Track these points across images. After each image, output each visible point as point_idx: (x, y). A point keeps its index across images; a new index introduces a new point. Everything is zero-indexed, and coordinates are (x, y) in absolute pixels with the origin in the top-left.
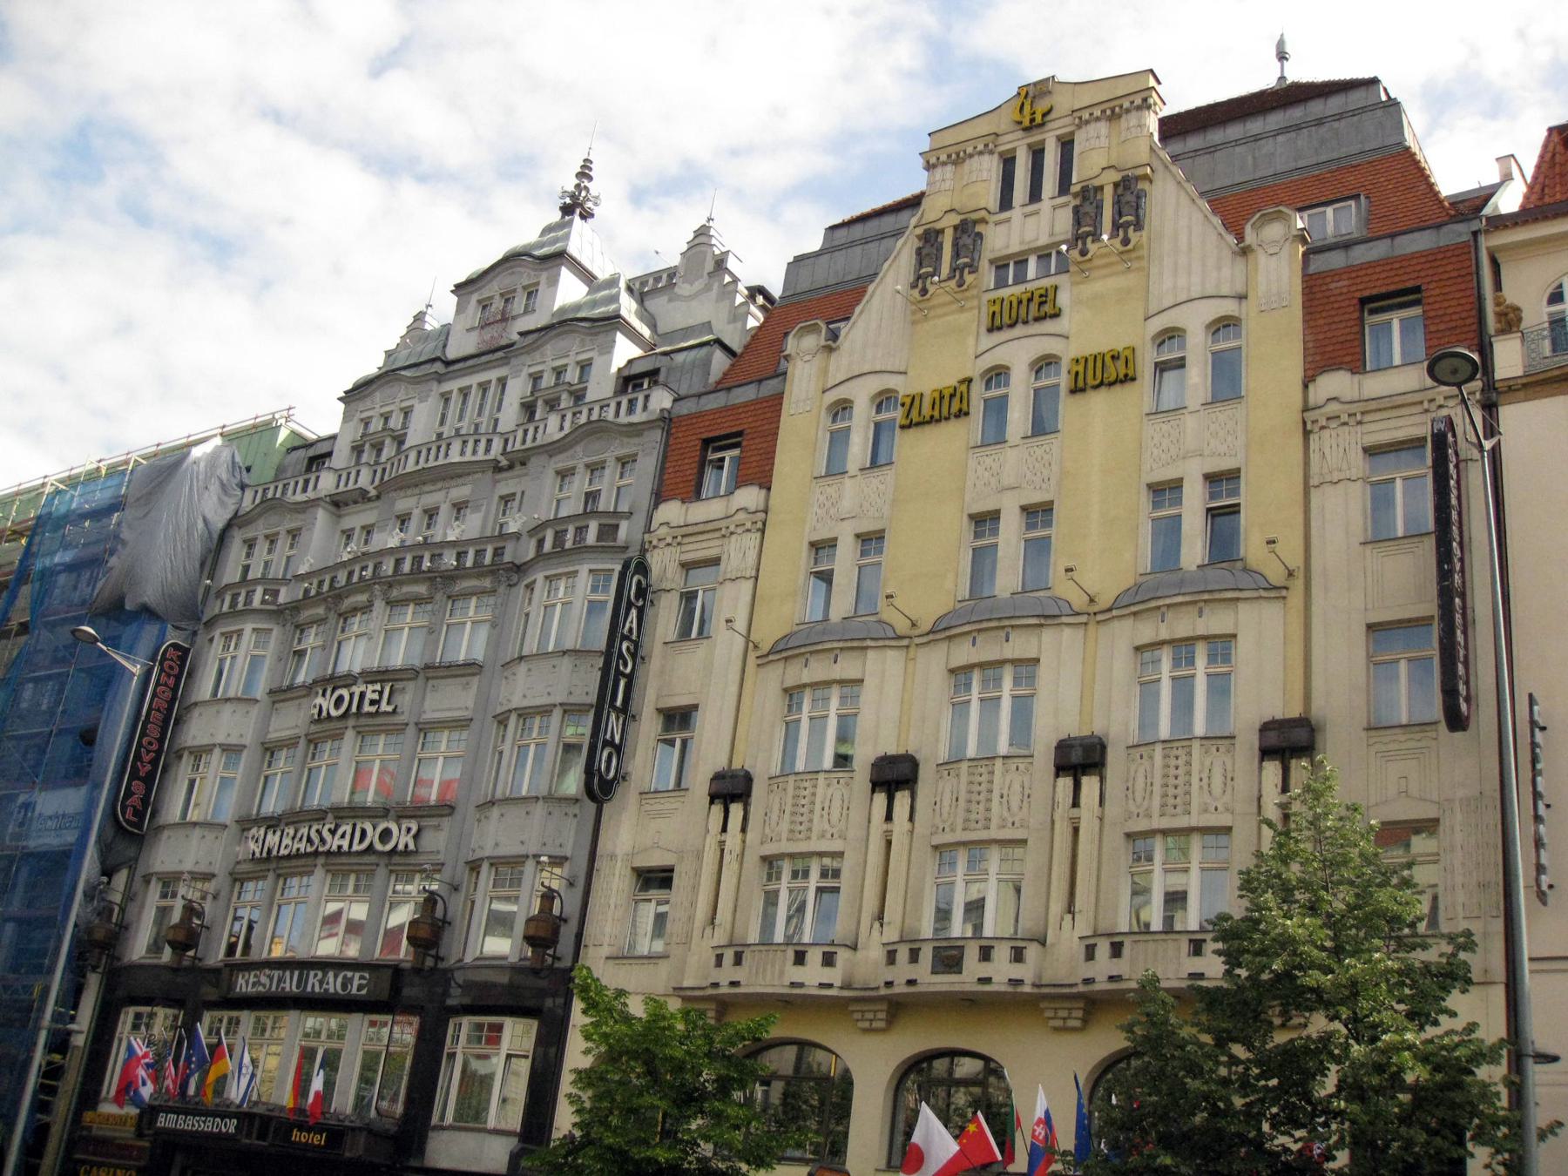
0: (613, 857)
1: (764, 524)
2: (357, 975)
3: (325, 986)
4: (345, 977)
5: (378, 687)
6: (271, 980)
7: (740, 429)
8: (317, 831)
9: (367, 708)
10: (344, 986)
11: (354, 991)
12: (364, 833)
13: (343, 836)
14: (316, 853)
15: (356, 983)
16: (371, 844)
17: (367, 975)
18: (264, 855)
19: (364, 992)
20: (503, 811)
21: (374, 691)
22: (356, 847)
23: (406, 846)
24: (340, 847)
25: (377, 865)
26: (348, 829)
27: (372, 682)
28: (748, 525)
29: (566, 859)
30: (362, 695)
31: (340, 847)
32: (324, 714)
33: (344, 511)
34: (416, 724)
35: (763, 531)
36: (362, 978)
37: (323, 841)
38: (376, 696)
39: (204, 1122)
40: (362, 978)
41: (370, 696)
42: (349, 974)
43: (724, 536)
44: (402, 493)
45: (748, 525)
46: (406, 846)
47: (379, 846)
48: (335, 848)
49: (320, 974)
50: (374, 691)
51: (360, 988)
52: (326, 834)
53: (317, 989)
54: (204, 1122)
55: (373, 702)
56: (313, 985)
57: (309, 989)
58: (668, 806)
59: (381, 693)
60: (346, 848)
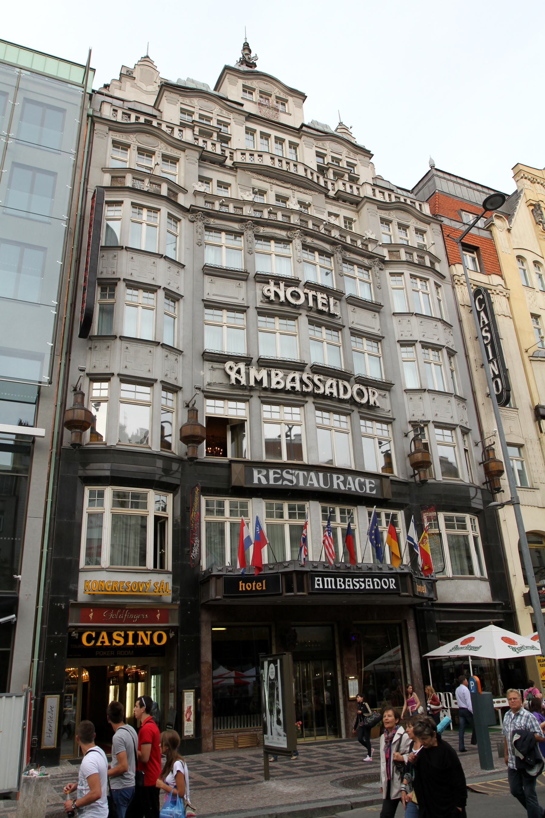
2: (367, 481)
3: (348, 486)
4: (359, 480)
6: (297, 477)
10: (361, 488)
11: (368, 491)
13: (331, 386)
15: (368, 486)
16: (352, 396)
17: (373, 481)
18: (252, 383)
19: (374, 492)
20: (411, 396)
22: (342, 396)
23: (375, 403)
25: (353, 411)
30: (315, 299)
31: (331, 393)
36: (370, 483)
37: (318, 388)
39: (364, 582)
40: (370, 483)
41: (320, 301)
42: (362, 480)
46: (375, 403)
47: (357, 399)
49: (342, 478)
50: (322, 298)
51: (371, 489)
53: (342, 487)
54: (364, 582)
55: (323, 304)
56: (338, 484)
57: (335, 487)
60: (335, 394)
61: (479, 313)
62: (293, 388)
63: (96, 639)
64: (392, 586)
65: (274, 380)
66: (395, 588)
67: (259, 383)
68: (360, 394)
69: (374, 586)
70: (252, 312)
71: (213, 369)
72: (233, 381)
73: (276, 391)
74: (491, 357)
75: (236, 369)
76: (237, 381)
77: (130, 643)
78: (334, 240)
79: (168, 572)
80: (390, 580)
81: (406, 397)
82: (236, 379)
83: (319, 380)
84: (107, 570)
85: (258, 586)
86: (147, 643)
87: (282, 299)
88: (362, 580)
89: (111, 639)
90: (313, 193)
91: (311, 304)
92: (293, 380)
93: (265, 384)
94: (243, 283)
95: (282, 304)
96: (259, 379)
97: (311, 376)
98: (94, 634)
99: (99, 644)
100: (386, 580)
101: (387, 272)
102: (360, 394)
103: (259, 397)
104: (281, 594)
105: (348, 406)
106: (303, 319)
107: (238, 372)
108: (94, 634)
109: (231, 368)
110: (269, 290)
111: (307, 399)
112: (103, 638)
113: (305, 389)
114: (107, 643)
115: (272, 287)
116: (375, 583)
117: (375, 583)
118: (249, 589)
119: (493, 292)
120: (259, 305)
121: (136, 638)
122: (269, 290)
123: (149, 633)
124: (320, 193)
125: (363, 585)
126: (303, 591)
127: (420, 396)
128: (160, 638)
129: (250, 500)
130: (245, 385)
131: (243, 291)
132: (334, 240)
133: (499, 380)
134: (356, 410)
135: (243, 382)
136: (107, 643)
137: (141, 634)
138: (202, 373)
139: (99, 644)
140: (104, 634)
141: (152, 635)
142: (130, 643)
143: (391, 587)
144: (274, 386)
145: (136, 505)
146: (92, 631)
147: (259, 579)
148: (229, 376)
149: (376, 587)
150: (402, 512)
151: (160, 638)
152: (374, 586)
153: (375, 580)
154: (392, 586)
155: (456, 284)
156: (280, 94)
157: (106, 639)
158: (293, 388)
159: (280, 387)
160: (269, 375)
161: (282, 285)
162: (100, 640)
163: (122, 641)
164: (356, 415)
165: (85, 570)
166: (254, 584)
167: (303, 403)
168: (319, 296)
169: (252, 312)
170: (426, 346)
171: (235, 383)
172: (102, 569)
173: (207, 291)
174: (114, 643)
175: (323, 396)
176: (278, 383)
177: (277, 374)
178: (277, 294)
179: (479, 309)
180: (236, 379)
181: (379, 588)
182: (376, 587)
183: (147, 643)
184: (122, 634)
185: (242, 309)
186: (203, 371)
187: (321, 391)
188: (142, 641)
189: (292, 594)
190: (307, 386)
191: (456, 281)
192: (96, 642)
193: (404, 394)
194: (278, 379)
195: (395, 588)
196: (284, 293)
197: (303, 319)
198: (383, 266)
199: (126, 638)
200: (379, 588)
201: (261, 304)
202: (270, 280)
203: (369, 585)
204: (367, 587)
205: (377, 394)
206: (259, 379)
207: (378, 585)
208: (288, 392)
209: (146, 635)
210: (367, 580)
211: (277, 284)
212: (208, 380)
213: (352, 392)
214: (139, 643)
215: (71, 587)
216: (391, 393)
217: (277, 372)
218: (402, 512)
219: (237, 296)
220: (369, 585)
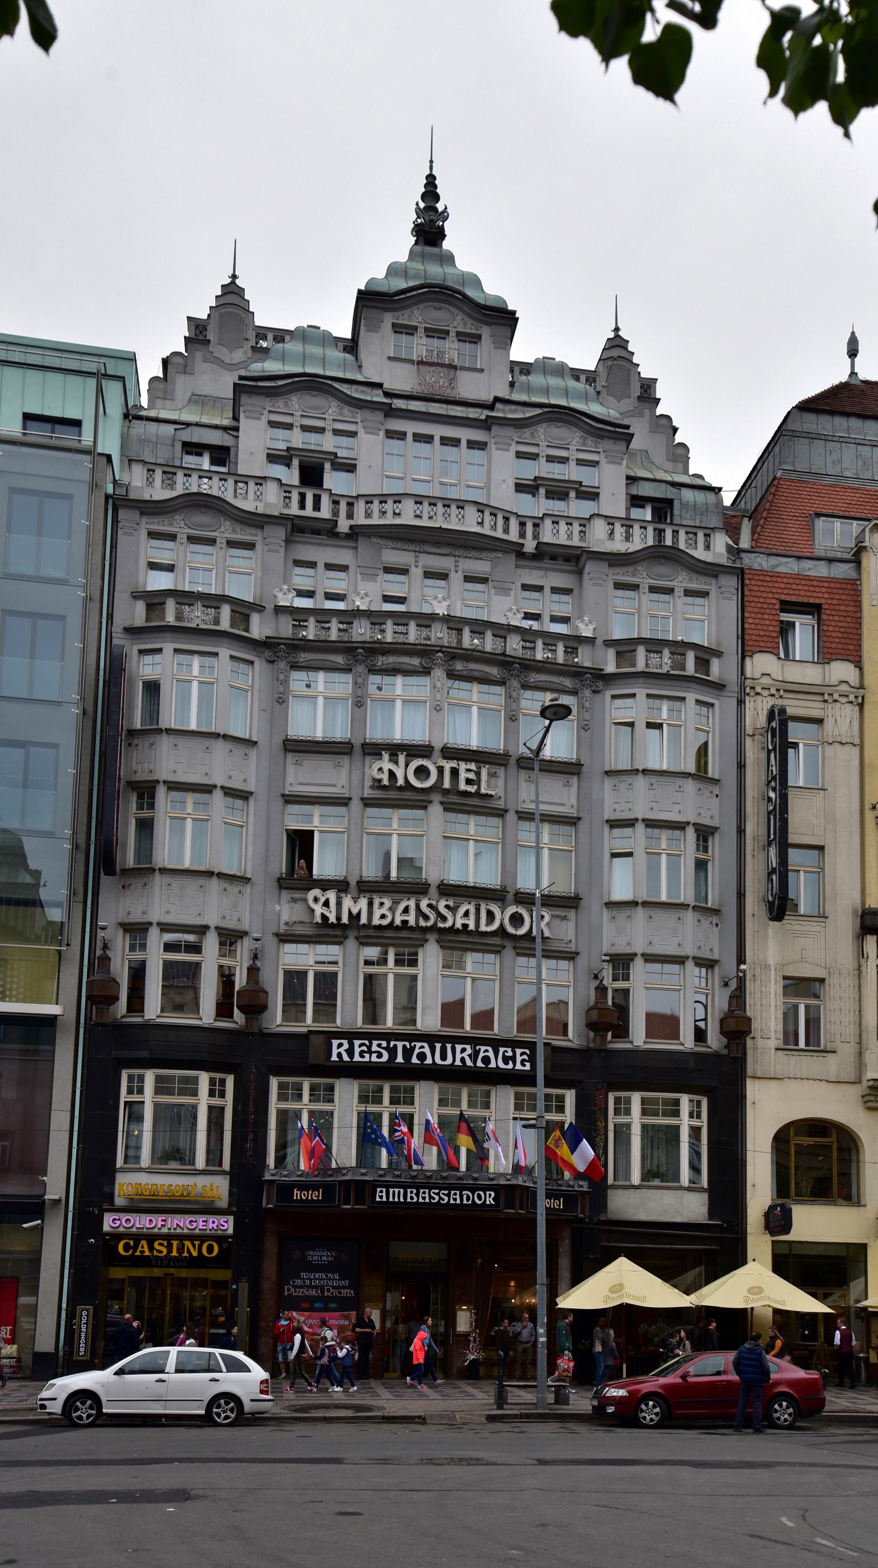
0: (767, 967)
1: (863, 698)
5: (473, 766)
7: (817, 601)
8: (430, 906)
9: (463, 786)
12: (491, 916)
13: (466, 914)
14: (434, 928)
16: (502, 926)
18: (345, 920)
21: (468, 770)
22: (483, 928)
24: (465, 926)
25: (504, 947)
26: (472, 908)
27: (467, 760)
28: (852, 698)
29: (716, 962)
30: (455, 772)
31: (465, 926)
32: (401, 782)
33: (298, 537)
34: (517, 812)
35: (861, 706)
37: (444, 919)
38: (472, 776)
39: (448, 1195)
41: (463, 775)
43: (826, 701)
44: (390, 543)
45: (852, 698)
47: (510, 930)
48: (458, 925)
50: (468, 770)
52: (441, 906)
54: (448, 1195)
55: (469, 782)
58: (808, 928)
59: (478, 774)
60: (472, 927)
61: (769, 752)
62: (405, 922)
63: (135, 1248)
64: (490, 1201)
65: (377, 913)
66: (493, 1203)
67: (355, 918)
68: (516, 920)
69: (462, 1199)
70: (356, 805)
71: (294, 900)
72: (318, 919)
73: (380, 927)
74: (772, 837)
75: (322, 900)
76: (324, 917)
77: (174, 1253)
78: (503, 658)
79: (224, 1173)
80: (488, 1193)
81: (606, 914)
82: (323, 915)
83: (447, 907)
84: (148, 1171)
85: (315, 1195)
86: (195, 1253)
87: (401, 782)
88: (446, 1192)
89: (151, 1248)
90: (494, 555)
91: (447, 784)
92: (406, 910)
93: (364, 920)
94: (345, 760)
95: (401, 788)
96: (355, 911)
97: (434, 902)
98: (132, 1243)
99: (138, 1253)
100: (482, 1193)
101: (609, 693)
102: (516, 920)
103: (357, 938)
104: (339, 1206)
105: (497, 941)
106: (436, 809)
107: (326, 904)
108: (132, 1243)
109: (316, 900)
110: (380, 769)
111: (428, 936)
112: (142, 1247)
113: (422, 923)
114: (147, 1253)
115: (386, 764)
116: (465, 1197)
117: (465, 1197)
118: (304, 1198)
119: (826, 697)
120: (368, 793)
121: (181, 1249)
122: (380, 769)
123: (197, 1243)
124: (505, 552)
125: (446, 1199)
126: (364, 1205)
127: (628, 913)
128: (210, 1249)
129: (338, 1081)
130: (335, 922)
131: (344, 772)
132: (503, 658)
133: (774, 877)
134: (509, 945)
135: (332, 919)
136: (147, 1253)
137: (188, 1244)
138: (277, 907)
139: (138, 1253)
140: (144, 1243)
141: (200, 1246)
142: (174, 1253)
143: (488, 1202)
144: (376, 921)
145: (183, 1092)
146: (130, 1239)
147: (314, 1186)
148: (313, 911)
149: (465, 1202)
150: (573, 1091)
151: (210, 1249)
152: (462, 1199)
153: (464, 1192)
154: (490, 1201)
155: (748, 694)
156: (465, 325)
157: (146, 1249)
158: (405, 922)
159: (385, 922)
160: (370, 904)
161: (402, 758)
162: (140, 1249)
163: (165, 1251)
164: (509, 953)
165: (123, 1170)
166: (310, 1192)
167: (421, 943)
168: (463, 766)
169: (356, 805)
170: (650, 824)
171: (319, 921)
172: (141, 1170)
173: (290, 779)
174: (155, 1253)
175: (452, 930)
176: (383, 916)
177: (382, 904)
178: (392, 774)
179: (770, 747)
180: (323, 915)
181: (470, 1202)
182: (465, 1202)
183: (195, 1253)
184: (165, 1243)
185: (343, 802)
186: (279, 905)
187: (449, 924)
188: (189, 1251)
189: (349, 1207)
190: (426, 918)
191: (748, 690)
192: (135, 1250)
193: (605, 910)
194: (384, 910)
195: (493, 1203)
196: (406, 771)
197: (436, 809)
198: (600, 685)
199: (169, 1247)
200: (470, 1202)
201: (371, 792)
202: (383, 753)
203: (455, 1200)
204: (452, 1202)
205: (547, 918)
206: (355, 911)
207: (468, 1199)
208: (398, 928)
209: (194, 1246)
210: (452, 1192)
211: (394, 760)
212: (285, 917)
213: (502, 920)
214: (186, 1254)
215: (106, 1189)
216: (579, 911)
217: (381, 900)
218: (573, 1091)
219: (334, 782)
220: (455, 1200)
